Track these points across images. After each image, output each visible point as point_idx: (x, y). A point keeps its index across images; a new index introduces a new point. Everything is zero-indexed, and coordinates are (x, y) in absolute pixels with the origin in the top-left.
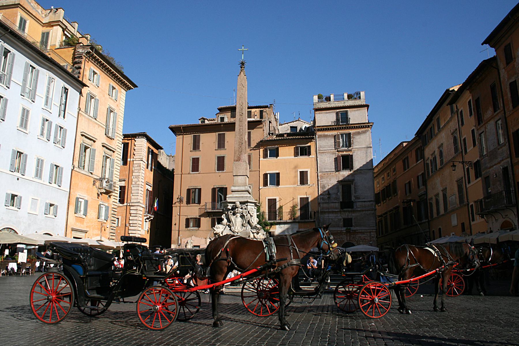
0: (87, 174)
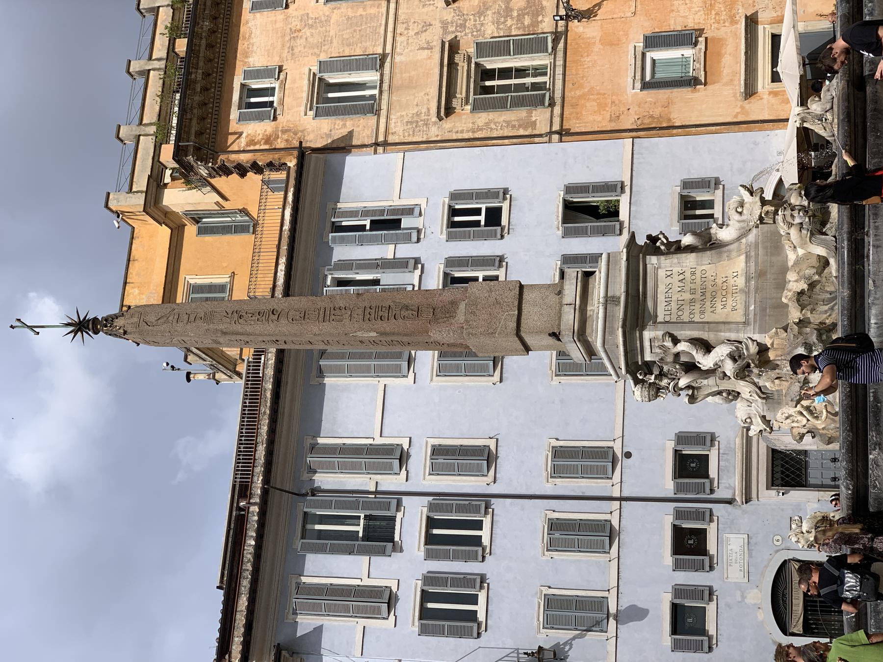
0: (560, 54)
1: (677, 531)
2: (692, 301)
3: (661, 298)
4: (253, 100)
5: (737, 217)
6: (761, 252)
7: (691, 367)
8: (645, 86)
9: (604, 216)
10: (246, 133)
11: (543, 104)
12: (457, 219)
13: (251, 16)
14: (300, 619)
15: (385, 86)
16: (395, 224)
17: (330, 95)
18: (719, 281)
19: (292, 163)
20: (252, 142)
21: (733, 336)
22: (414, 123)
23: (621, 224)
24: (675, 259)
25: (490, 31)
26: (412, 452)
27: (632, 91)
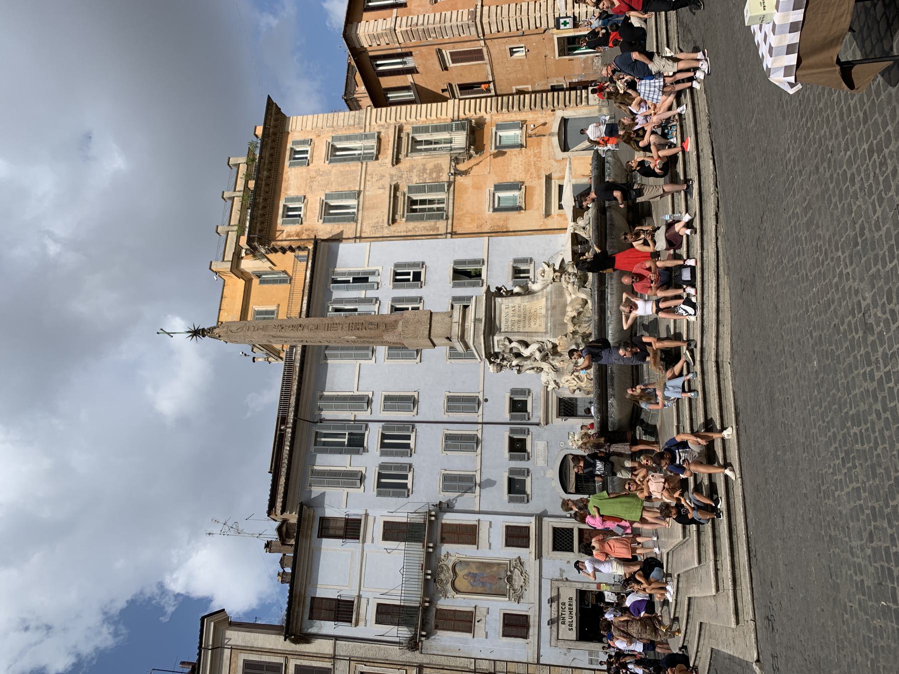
1: (512, 441)
2: (519, 321)
3: (503, 319)
4: (290, 213)
5: (541, 278)
6: (554, 296)
7: (518, 355)
8: (495, 210)
9: (474, 277)
10: (286, 230)
11: (442, 218)
12: (398, 277)
13: (289, 170)
14: (313, 489)
15: (360, 207)
16: (365, 280)
17: (331, 212)
18: (533, 311)
19: (311, 247)
20: (289, 235)
21: (540, 339)
22: (375, 227)
23: (483, 281)
24: (510, 299)
25: (415, 180)
26: (374, 399)
27: (488, 213)
